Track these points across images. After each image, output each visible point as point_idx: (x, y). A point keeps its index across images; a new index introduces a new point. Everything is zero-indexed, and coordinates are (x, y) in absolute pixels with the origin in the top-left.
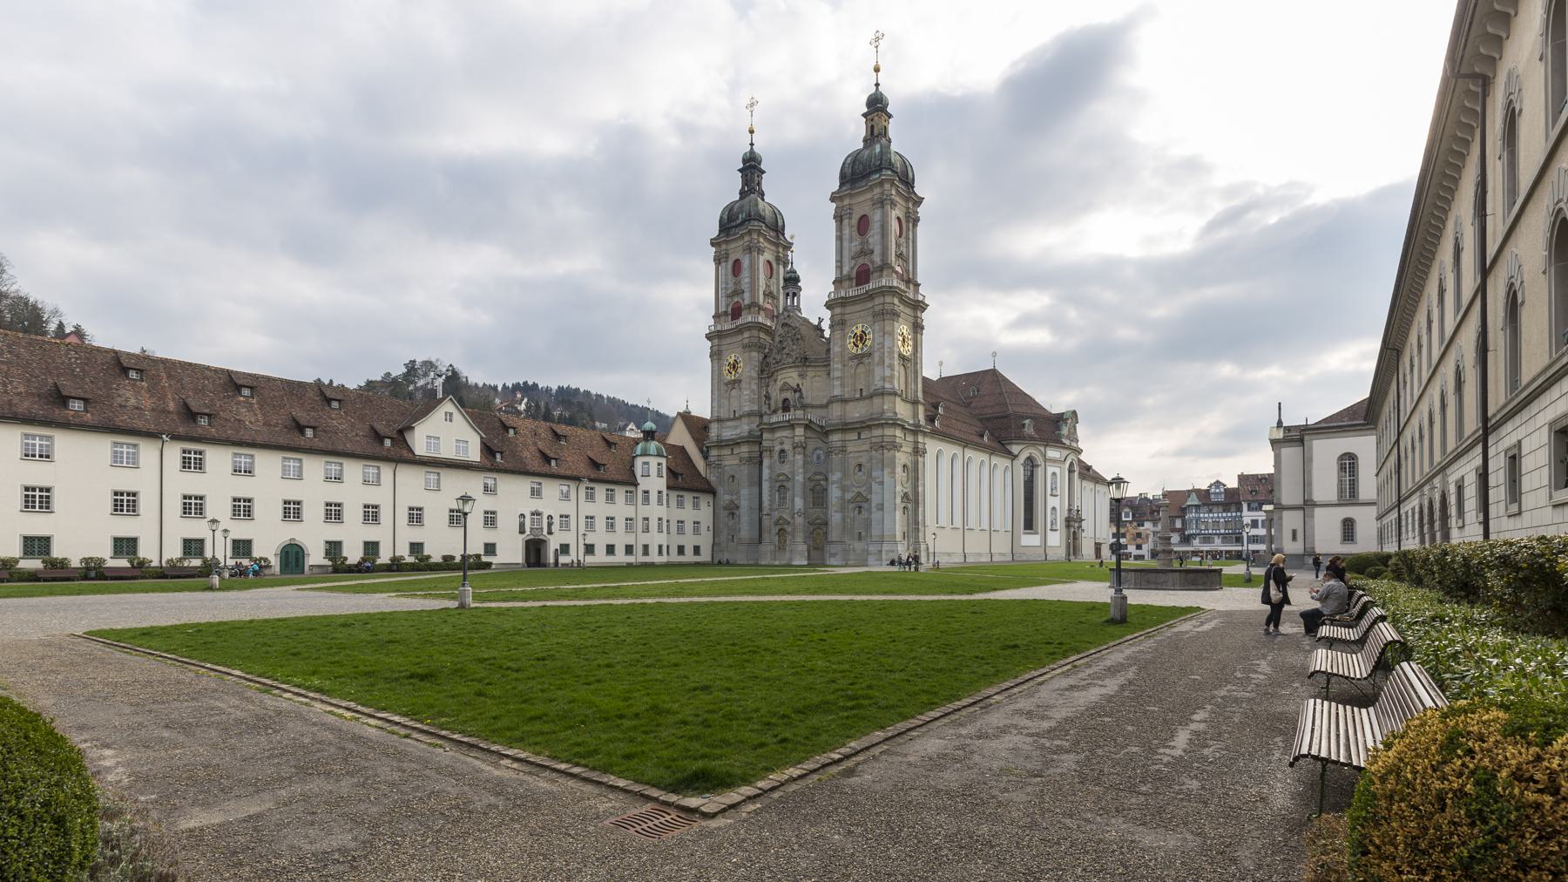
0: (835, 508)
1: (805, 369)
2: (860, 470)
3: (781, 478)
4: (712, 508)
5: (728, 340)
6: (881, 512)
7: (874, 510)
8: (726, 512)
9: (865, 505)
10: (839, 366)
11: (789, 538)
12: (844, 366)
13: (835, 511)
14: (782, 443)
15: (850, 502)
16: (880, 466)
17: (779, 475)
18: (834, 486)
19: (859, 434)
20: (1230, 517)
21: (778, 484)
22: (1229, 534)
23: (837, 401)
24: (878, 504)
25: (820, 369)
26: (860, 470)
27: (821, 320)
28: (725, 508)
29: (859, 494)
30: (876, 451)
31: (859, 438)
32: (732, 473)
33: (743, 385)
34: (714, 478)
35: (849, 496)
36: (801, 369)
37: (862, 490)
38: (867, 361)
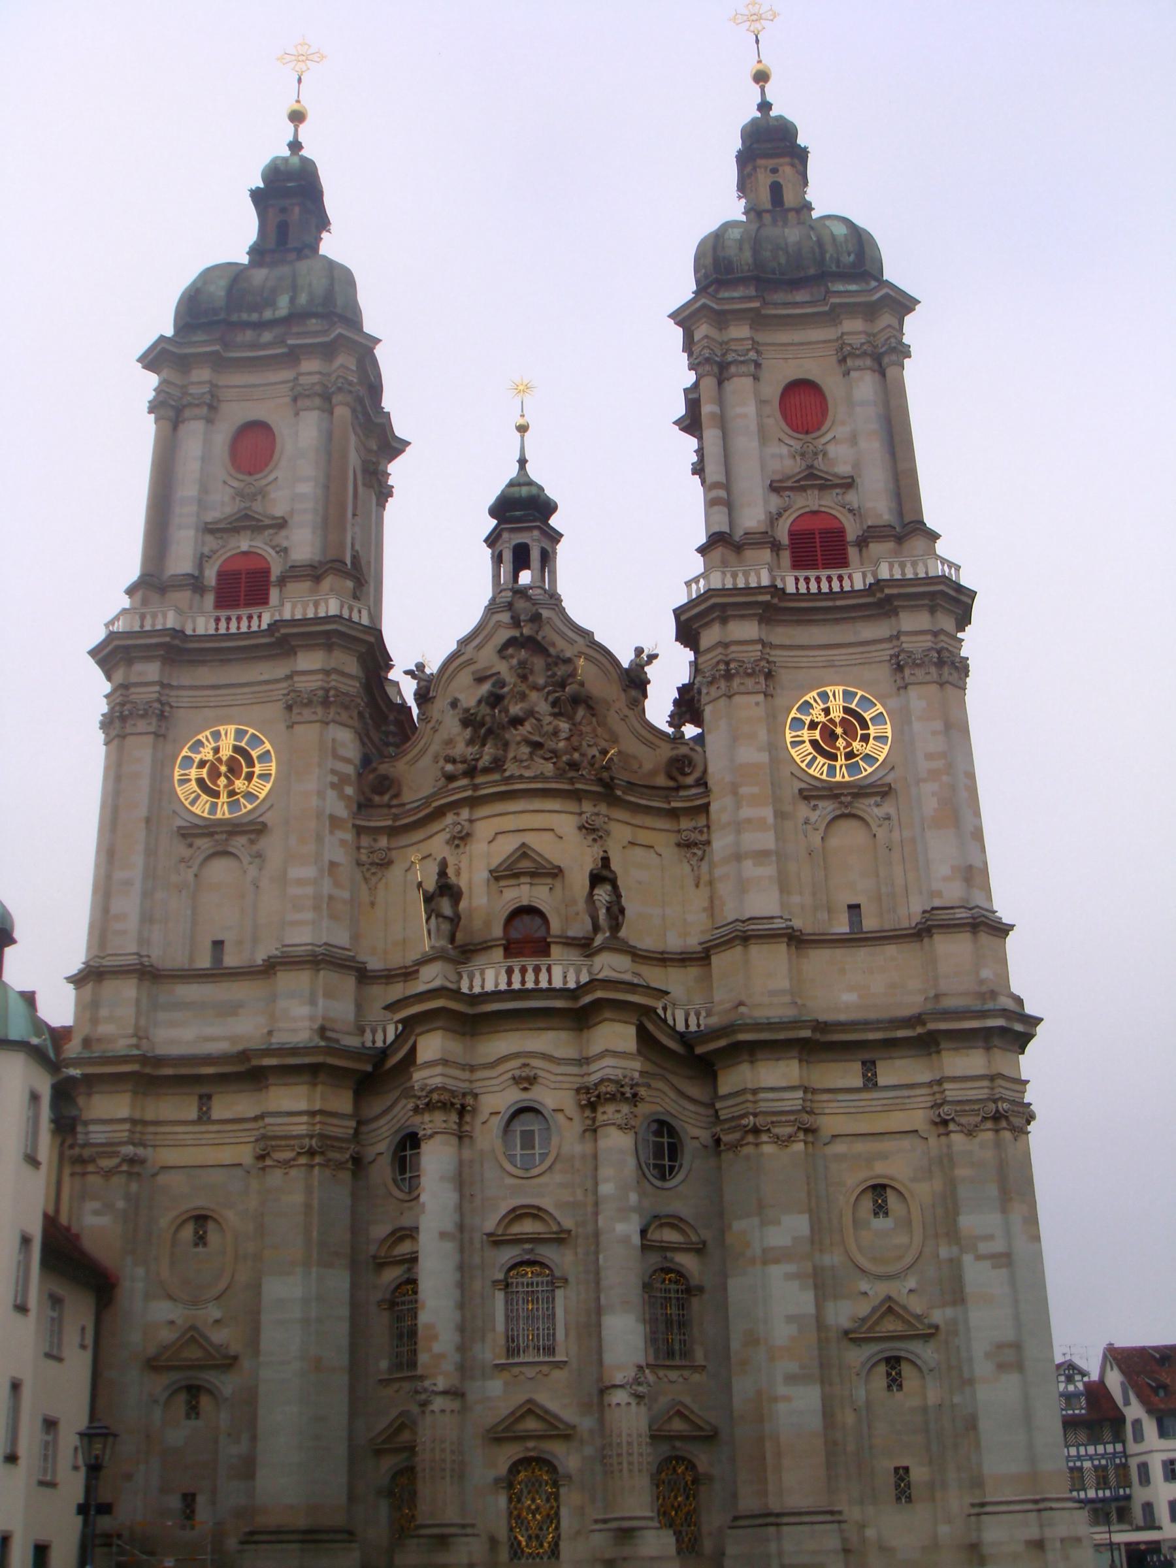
0: (793, 1367)
1: (603, 808)
2: (881, 1209)
3: (528, 1227)
4: (88, 1356)
5: (205, 675)
6: (1011, 1380)
7: (982, 1368)
8: (159, 1384)
9: (927, 1353)
10: (767, 813)
11: (570, 1499)
12: (780, 815)
13: (791, 1379)
14: (527, 1081)
15: (852, 1337)
16: (993, 1190)
17: (518, 1214)
18: (777, 1271)
19: (869, 1066)
20: (1103, 1456)
21: (508, 1255)
22: (1103, 1500)
23: (771, 936)
24: (1000, 1346)
25: (649, 821)
26: (881, 1209)
27: (644, 658)
28: (153, 1365)
29: (889, 1308)
30: (970, 1133)
31: (871, 1083)
32: (200, 1202)
33: (272, 845)
34: (104, 1221)
35: (842, 1314)
36: (587, 807)
37: (900, 1290)
38: (876, 810)
